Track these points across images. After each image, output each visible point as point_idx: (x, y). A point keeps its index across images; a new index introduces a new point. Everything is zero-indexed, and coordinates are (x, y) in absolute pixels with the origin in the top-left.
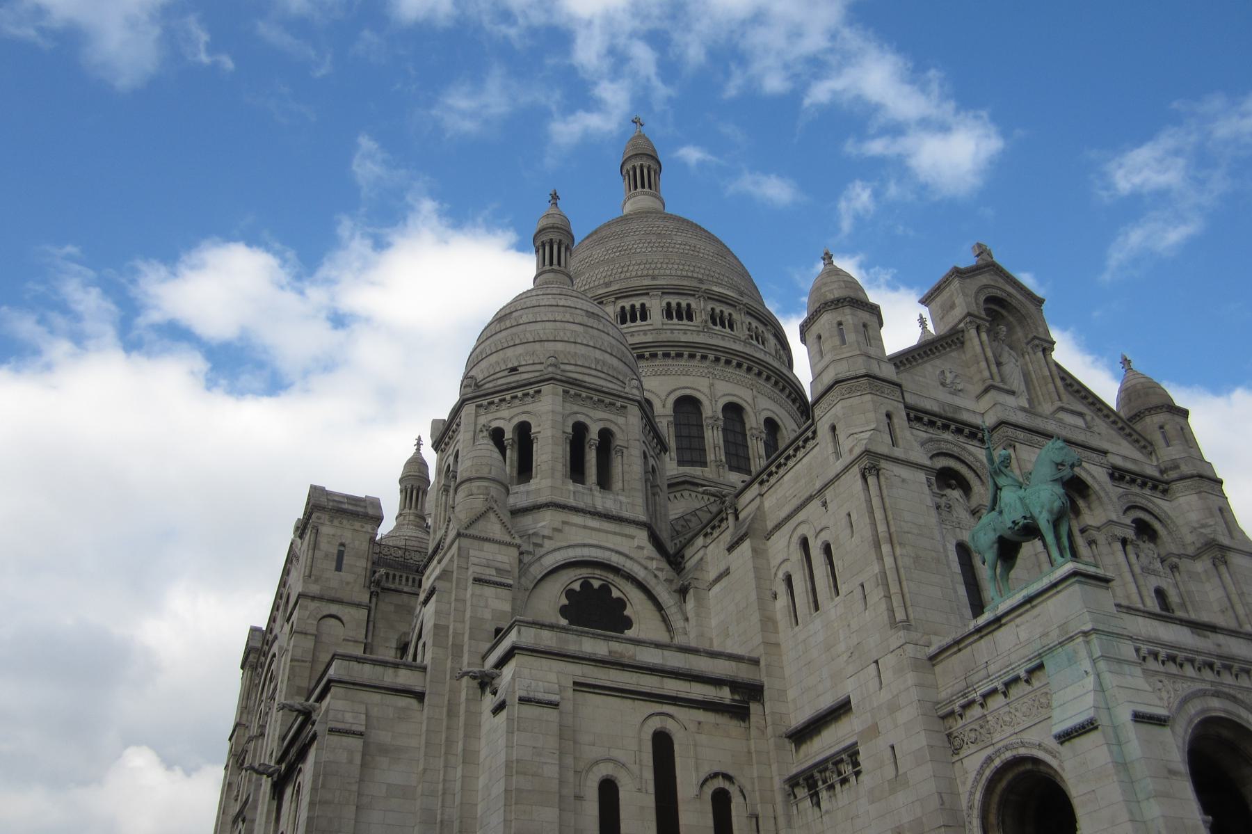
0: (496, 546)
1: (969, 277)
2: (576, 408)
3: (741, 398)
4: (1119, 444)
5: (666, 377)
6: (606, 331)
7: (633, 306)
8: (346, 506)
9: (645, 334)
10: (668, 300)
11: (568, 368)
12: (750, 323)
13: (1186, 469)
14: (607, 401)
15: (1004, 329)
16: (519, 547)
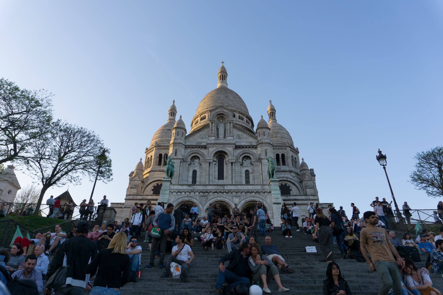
2: (160, 151)
4: (249, 139)
11: (161, 143)
13: (260, 142)
15: (221, 120)
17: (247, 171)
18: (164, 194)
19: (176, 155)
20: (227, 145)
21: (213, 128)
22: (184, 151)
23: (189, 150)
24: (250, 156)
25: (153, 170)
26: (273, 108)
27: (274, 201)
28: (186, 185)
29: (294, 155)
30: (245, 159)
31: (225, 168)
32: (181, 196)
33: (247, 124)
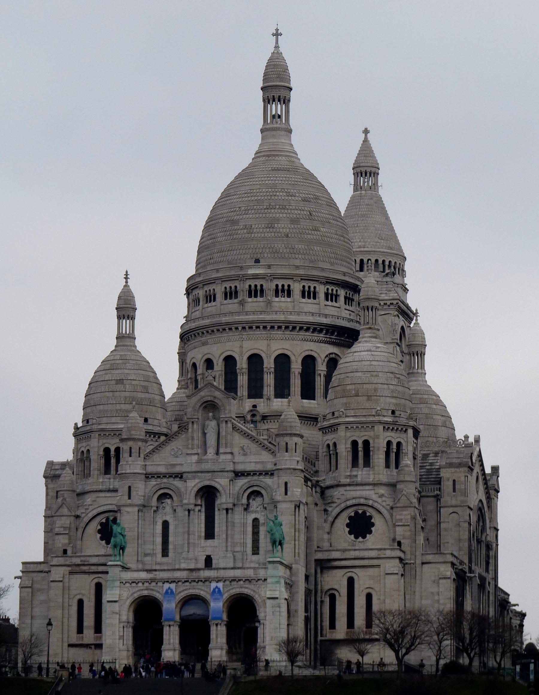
0: (66, 517)
1: (195, 396)
2: (105, 441)
3: (259, 349)
4: (260, 454)
5: (218, 345)
6: (124, 390)
7: (210, 290)
8: (57, 472)
9: (208, 318)
10: (224, 286)
11: (105, 420)
12: (277, 286)
14: (117, 434)
15: (211, 414)
16: (74, 516)
17: (256, 520)
18: (113, 587)
19: (129, 498)
20: (219, 473)
21: (195, 435)
22: (143, 487)
23: (153, 482)
24: (262, 492)
25: (95, 487)
26: (370, 293)
27: (269, 594)
28: (144, 571)
29: (398, 435)
30: (253, 497)
31: (216, 517)
32: (137, 589)
33: (329, 303)
